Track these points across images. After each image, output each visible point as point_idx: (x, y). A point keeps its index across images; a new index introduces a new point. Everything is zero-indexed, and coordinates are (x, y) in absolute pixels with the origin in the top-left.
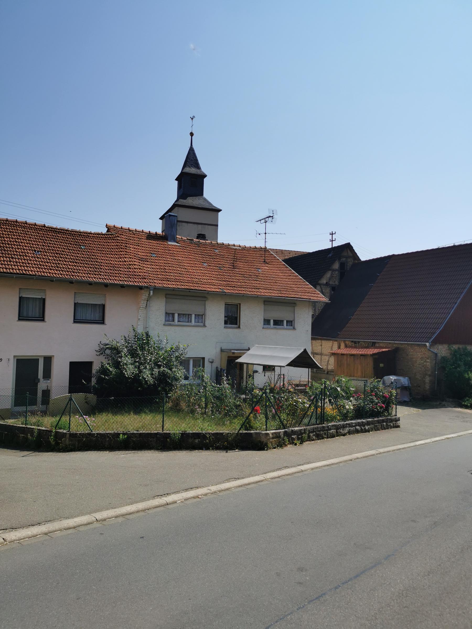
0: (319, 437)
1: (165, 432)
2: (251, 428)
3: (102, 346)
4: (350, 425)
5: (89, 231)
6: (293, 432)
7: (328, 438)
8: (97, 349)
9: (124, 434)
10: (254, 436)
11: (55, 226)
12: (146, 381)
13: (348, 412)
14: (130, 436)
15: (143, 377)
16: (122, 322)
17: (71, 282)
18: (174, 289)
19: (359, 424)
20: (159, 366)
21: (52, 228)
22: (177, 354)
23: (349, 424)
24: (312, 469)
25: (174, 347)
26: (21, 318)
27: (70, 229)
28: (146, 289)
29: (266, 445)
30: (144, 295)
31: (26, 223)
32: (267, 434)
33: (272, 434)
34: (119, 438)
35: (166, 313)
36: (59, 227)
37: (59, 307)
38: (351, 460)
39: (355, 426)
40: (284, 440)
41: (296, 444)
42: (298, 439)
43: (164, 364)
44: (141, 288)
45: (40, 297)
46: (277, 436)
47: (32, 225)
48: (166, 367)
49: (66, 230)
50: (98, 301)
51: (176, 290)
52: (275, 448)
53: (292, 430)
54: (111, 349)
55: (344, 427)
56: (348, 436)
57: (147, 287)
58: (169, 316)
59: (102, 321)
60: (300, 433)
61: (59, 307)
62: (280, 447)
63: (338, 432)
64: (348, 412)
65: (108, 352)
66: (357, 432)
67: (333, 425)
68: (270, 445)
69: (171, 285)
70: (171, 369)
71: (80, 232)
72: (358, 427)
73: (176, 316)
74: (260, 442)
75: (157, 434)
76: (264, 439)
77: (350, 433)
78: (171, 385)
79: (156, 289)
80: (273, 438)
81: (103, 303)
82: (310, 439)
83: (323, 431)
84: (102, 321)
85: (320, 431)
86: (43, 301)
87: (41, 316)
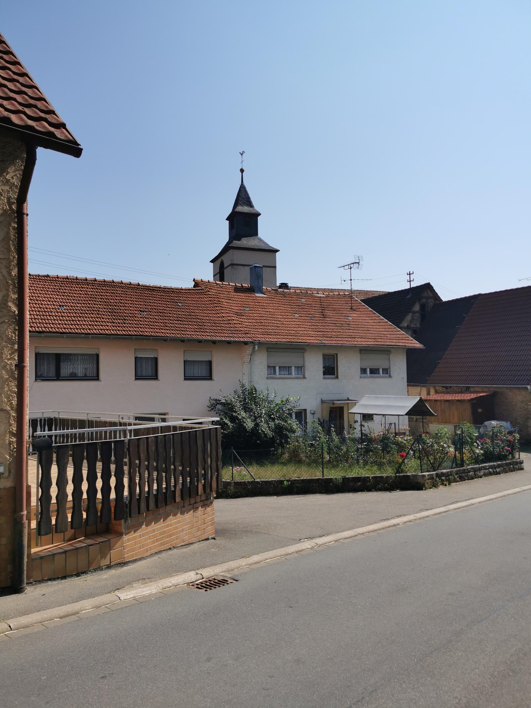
0: (462, 479)
1: (324, 477)
2: (402, 471)
3: (213, 402)
4: (485, 468)
5: (180, 287)
6: (443, 474)
7: (468, 480)
8: (209, 404)
9: (288, 481)
10: (411, 478)
11: (148, 284)
12: (265, 435)
13: (478, 456)
14: (293, 482)
15: (262, 430)
16: (230, 378)
17: (183, 341)
18: (276, 343)
19: (491, 467)
20: (273, 419)
21: (146, 286)
22: (289, 407)
23: (484, 467)
24: (479, 503)
25: (284, 399)
26: (138, 377)
27: (162, 286)
28: (250, 344)
29: (424, 485)
30: (249, 349)
31: (113, 282)
32: (424, 476)
33: (428, 475)
34: (284, 484)
35: (268, 366)
36: (152, 285)
37: (171, 364)
38: (504, 496)
39: (488, 469)
40: (436, 481)
41: (446, 485)
42: (447, 480)
43: (277, 416)
44: (246, 343)
45: (153, 356)
46: (431, 477)
47: (127, 284)
48: (280, 420)
49: (159, 288)
50: (205, 358)
51: (279, 344)
52: (431, 488)
53: (442, 473)
54: (223, 404)
55: (480, 469)
56: (483, 478)
57: (252, 342)
58: (271, 368)
59: (210, 377)
60: (447, 475)
61: (171, 364)
62: (435, 487)
63: (474, 475)
64: (478, 456)
65: (219, 407)
66: (490, 474)
67: (471, 468)
68: (427, 485)
69: (273, 339)
70: (286, 421)
71: (172, 289)
72: (491, 470)
73: (277, 369)
74: (418, 483)
75: (319, 479)
76: (420, 480)
77: (485, 475)
78: (287, 437)
79: (260, 344)
80: (429, 479)
81: (210, 359)
82: (455, 481)
83: (464, 473)
84: (210, 377)
85: (462, 473)
86: (156, 360)
87: (154, 375)
